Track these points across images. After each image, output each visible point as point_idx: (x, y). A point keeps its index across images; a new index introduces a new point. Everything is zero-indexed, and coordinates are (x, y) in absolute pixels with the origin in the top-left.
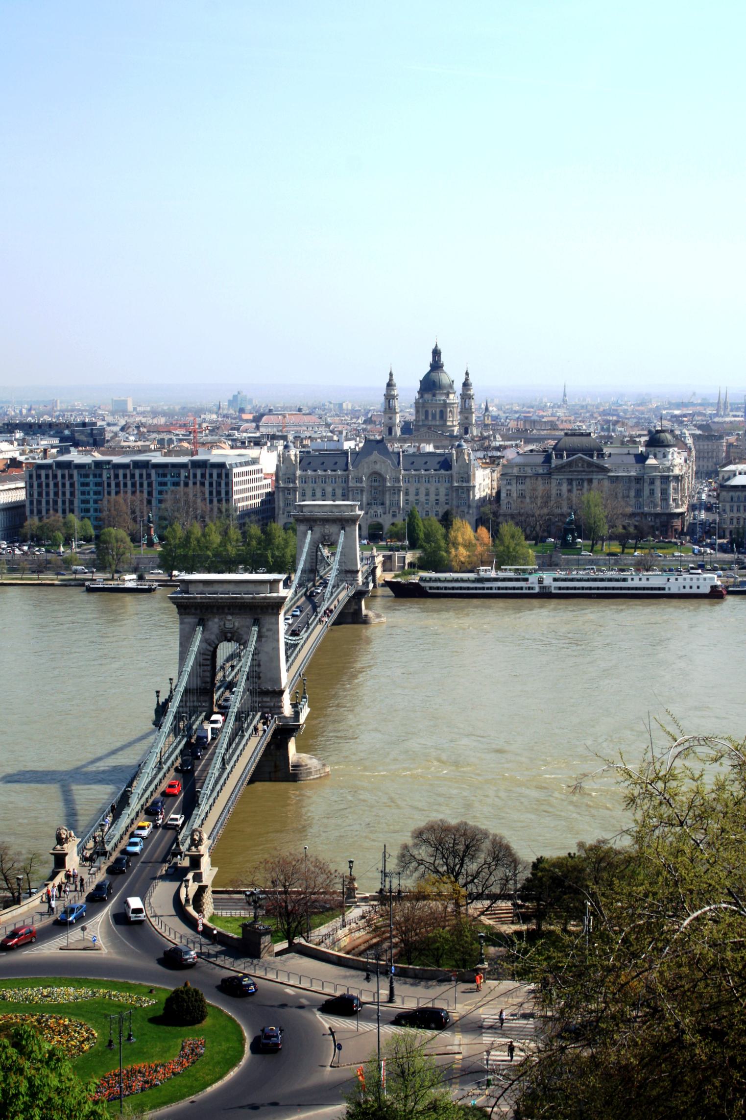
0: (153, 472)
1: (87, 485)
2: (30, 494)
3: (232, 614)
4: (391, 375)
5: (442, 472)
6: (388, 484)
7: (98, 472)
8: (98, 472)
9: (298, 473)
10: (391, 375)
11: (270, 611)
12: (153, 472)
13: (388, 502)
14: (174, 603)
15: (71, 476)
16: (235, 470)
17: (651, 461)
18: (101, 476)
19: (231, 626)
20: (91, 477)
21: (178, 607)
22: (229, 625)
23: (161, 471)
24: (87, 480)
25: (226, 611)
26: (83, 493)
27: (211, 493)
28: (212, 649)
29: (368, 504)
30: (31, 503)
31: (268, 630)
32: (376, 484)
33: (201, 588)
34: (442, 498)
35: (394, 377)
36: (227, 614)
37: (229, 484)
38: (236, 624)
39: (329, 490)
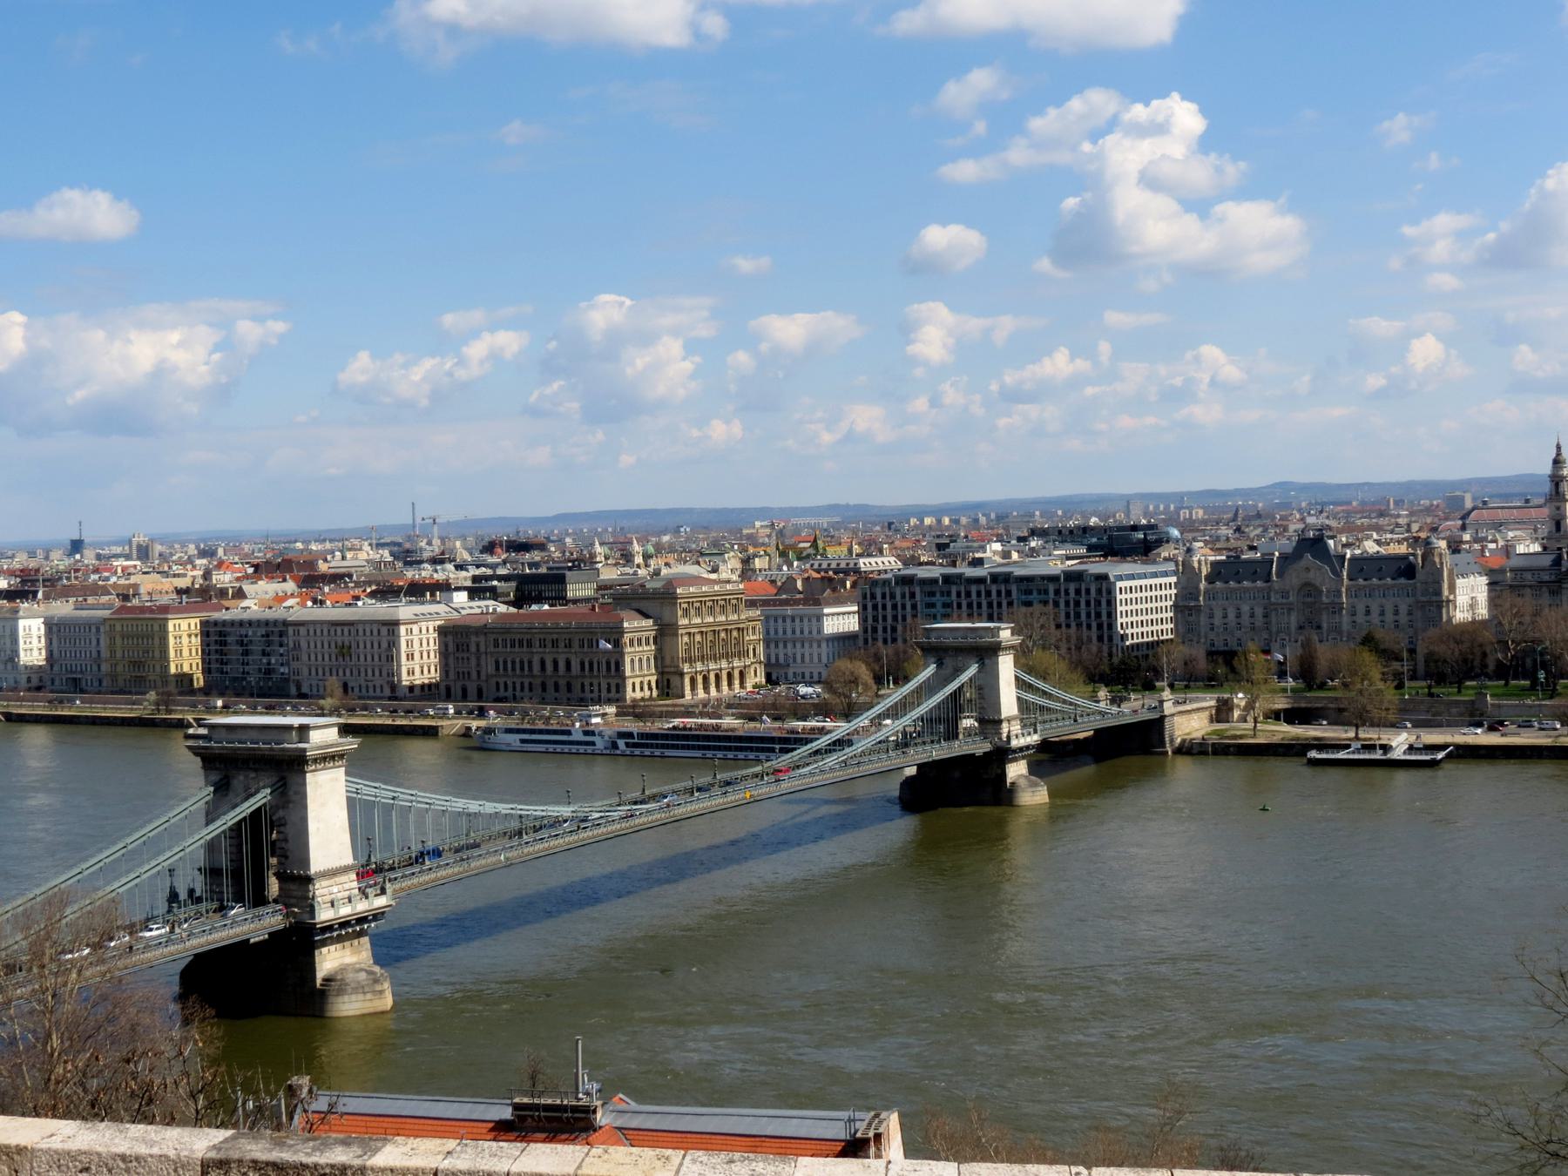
0: (1014, 588)
2: (863, 620)
3: (256, 770)
4: (1559, 447)
5: (1402, 581)
6: (1324, 599)
9: (1203, 585)
10: (1559, 447)
12: (1014, 588)
13: (1325, 625)
14: (196, 754)
15: (913, 595)
16: (1119, 584)
18: (949, 594)
21: (204, 760)
23: (1024, 586)
24: (933, 599)
27: (1088, 615)
29: (1301, 628)
30: (865, 631)
31: (296, 793)
33: (223, 734)
34: (1403, 618)
35: (1563, 451)
37: (1111, 603)
39: (1245, 608)
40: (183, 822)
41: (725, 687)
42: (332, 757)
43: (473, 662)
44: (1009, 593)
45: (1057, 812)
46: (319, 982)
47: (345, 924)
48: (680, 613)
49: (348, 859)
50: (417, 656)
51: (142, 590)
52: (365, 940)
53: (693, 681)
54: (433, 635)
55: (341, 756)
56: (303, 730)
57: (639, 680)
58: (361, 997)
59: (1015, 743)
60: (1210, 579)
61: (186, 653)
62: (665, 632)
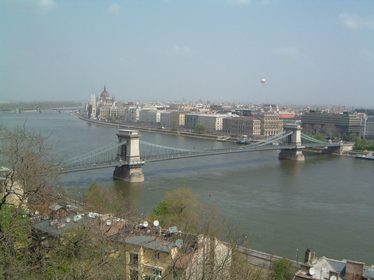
33: (121, 132)
40: (115, 145)
41: (276, 134)
42: (136, 137)
43: (228, 125)
45: (307, 162)
46: (130, 174)
47: (136, 165)
48: (265, 119)
49: (139, 155)
50: (219, 124)
51: (184, 109)
52: (141, 169)
53: (266, 132)
54: (222, 120)
55: (138, 137)
56: (131, 132)
57: (256, 132)
58: (136, 177)
59: (298, 147)
60: (367, 121)
61: (183, 121)
62: (262, 123)
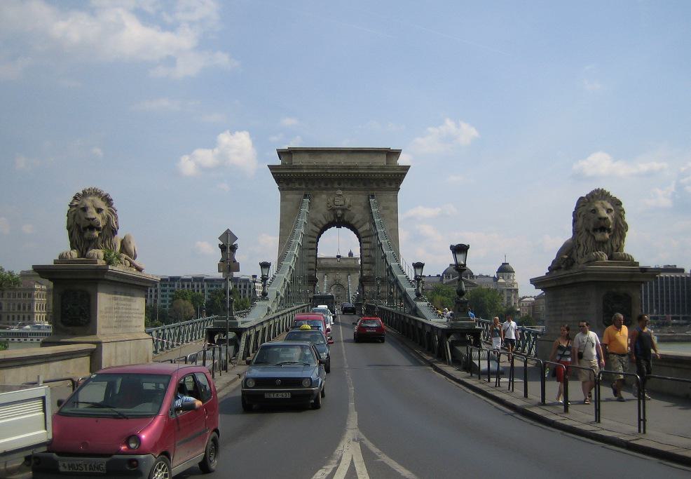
1: (165, 291)
3: (343, 189)
7: (172, 283)
8: (172, 283)
11: (388, 186)
17: (501, 280)
18: (174, 286)
19: (342, 203)
20: (168, 287)
22: (339, 202)
25: (336, 186)
26: (163, 296)
28: (319, 230)
32: (339, 293)
36: (337, 189)
38: (348, 201)
44: (203, 286)
